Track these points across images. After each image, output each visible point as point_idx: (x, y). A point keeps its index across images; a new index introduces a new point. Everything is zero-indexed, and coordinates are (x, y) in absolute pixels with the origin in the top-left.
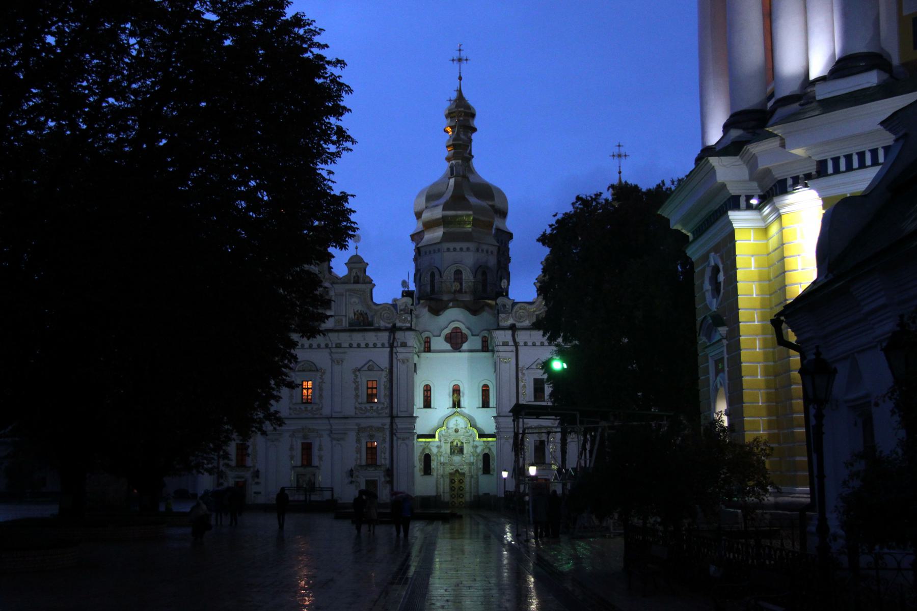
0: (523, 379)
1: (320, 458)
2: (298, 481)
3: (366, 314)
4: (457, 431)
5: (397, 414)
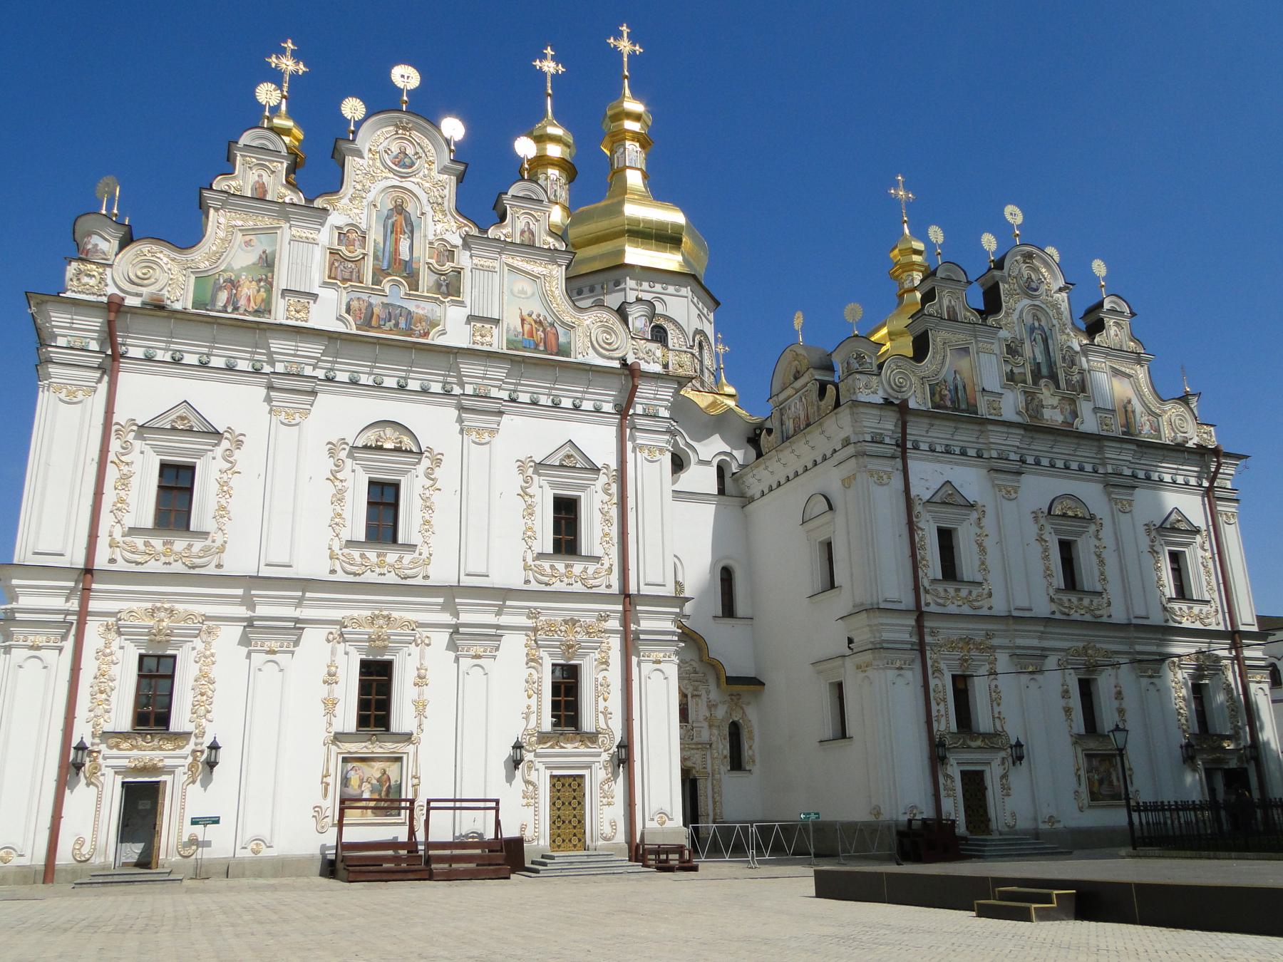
0: (919, 525)
1: (421, 708)
2: (345, 781)
3: (552, 325)
5: (639, 590)
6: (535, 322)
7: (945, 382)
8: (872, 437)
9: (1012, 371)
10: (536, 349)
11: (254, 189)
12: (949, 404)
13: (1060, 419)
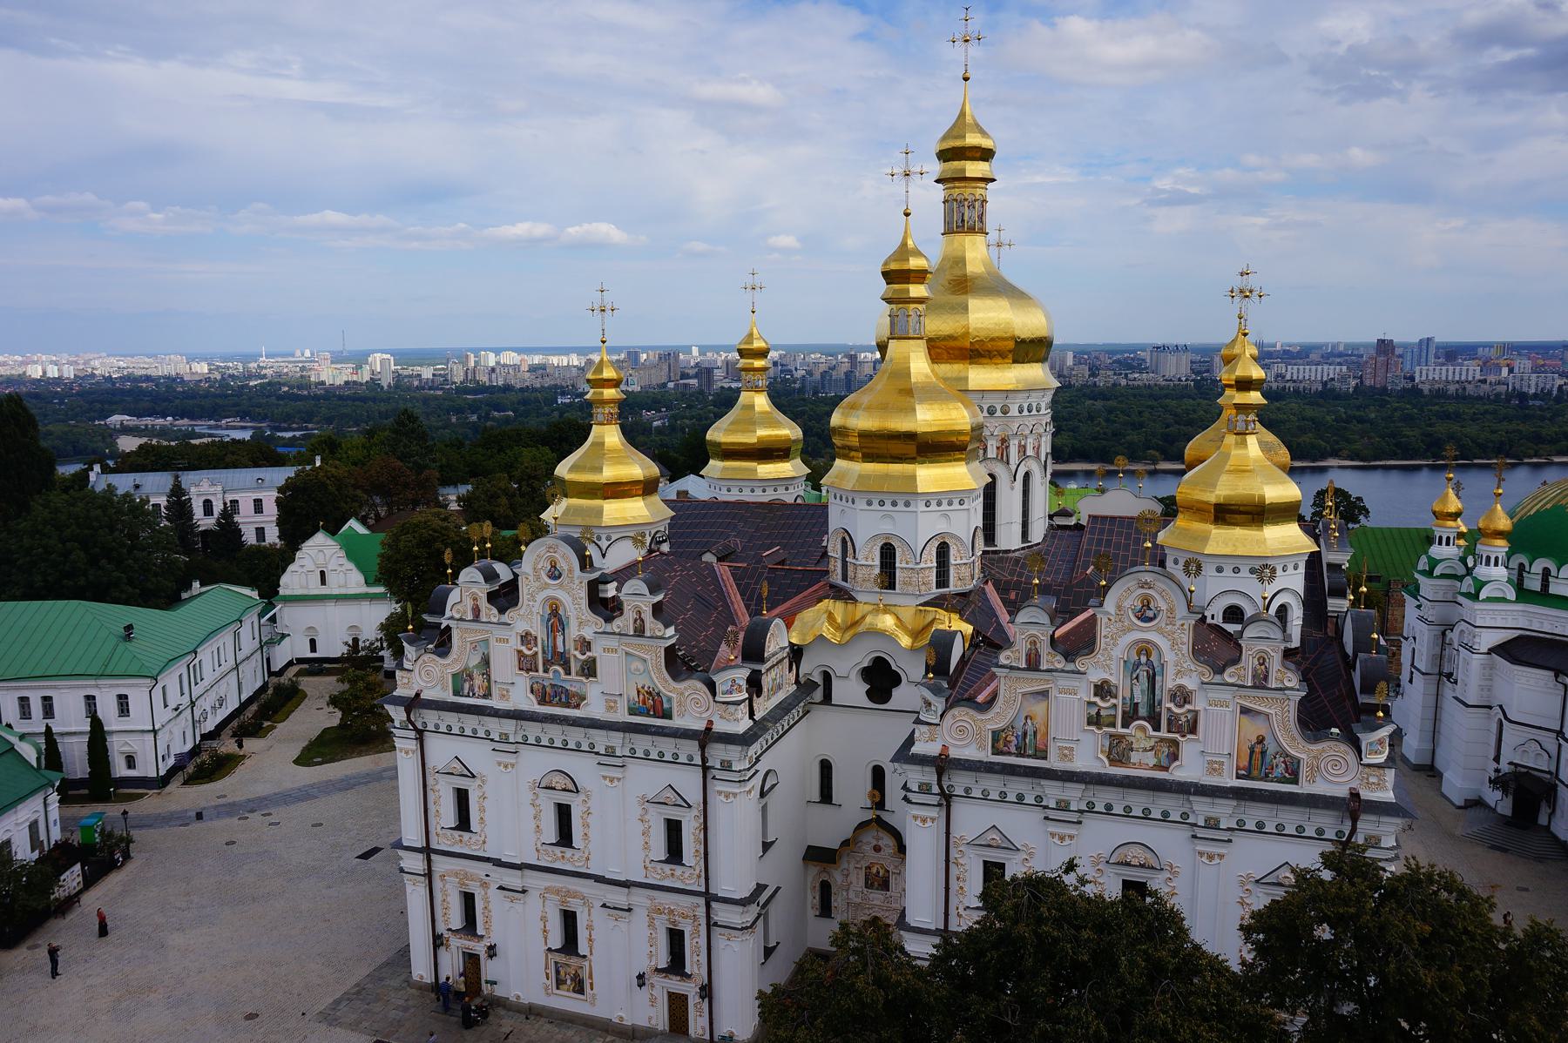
0: (960, 861)
3: (658, 694)
4: (877, 849)
6: (647, 692)
7: (1013, 728)
8: (919, 786)
9: (1098, 713)
10: (648, 715)
11: (473, 609)
12: (1013, 750)
13: (1152, 761)
